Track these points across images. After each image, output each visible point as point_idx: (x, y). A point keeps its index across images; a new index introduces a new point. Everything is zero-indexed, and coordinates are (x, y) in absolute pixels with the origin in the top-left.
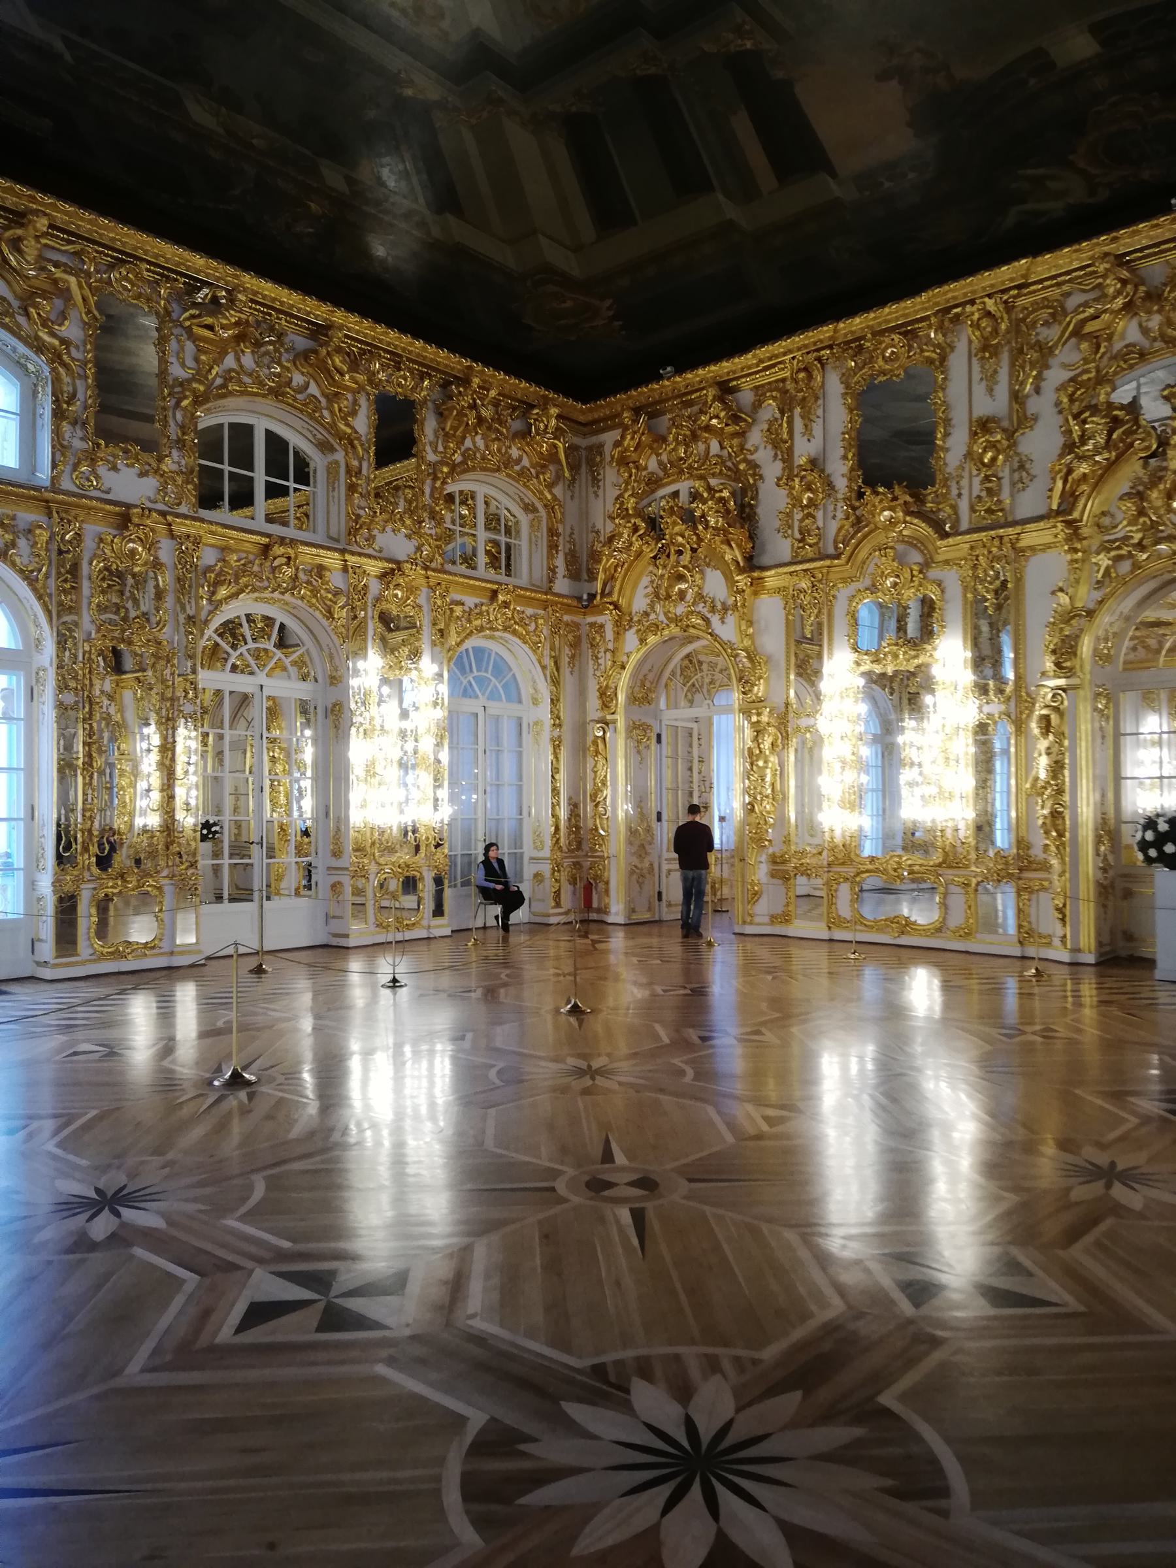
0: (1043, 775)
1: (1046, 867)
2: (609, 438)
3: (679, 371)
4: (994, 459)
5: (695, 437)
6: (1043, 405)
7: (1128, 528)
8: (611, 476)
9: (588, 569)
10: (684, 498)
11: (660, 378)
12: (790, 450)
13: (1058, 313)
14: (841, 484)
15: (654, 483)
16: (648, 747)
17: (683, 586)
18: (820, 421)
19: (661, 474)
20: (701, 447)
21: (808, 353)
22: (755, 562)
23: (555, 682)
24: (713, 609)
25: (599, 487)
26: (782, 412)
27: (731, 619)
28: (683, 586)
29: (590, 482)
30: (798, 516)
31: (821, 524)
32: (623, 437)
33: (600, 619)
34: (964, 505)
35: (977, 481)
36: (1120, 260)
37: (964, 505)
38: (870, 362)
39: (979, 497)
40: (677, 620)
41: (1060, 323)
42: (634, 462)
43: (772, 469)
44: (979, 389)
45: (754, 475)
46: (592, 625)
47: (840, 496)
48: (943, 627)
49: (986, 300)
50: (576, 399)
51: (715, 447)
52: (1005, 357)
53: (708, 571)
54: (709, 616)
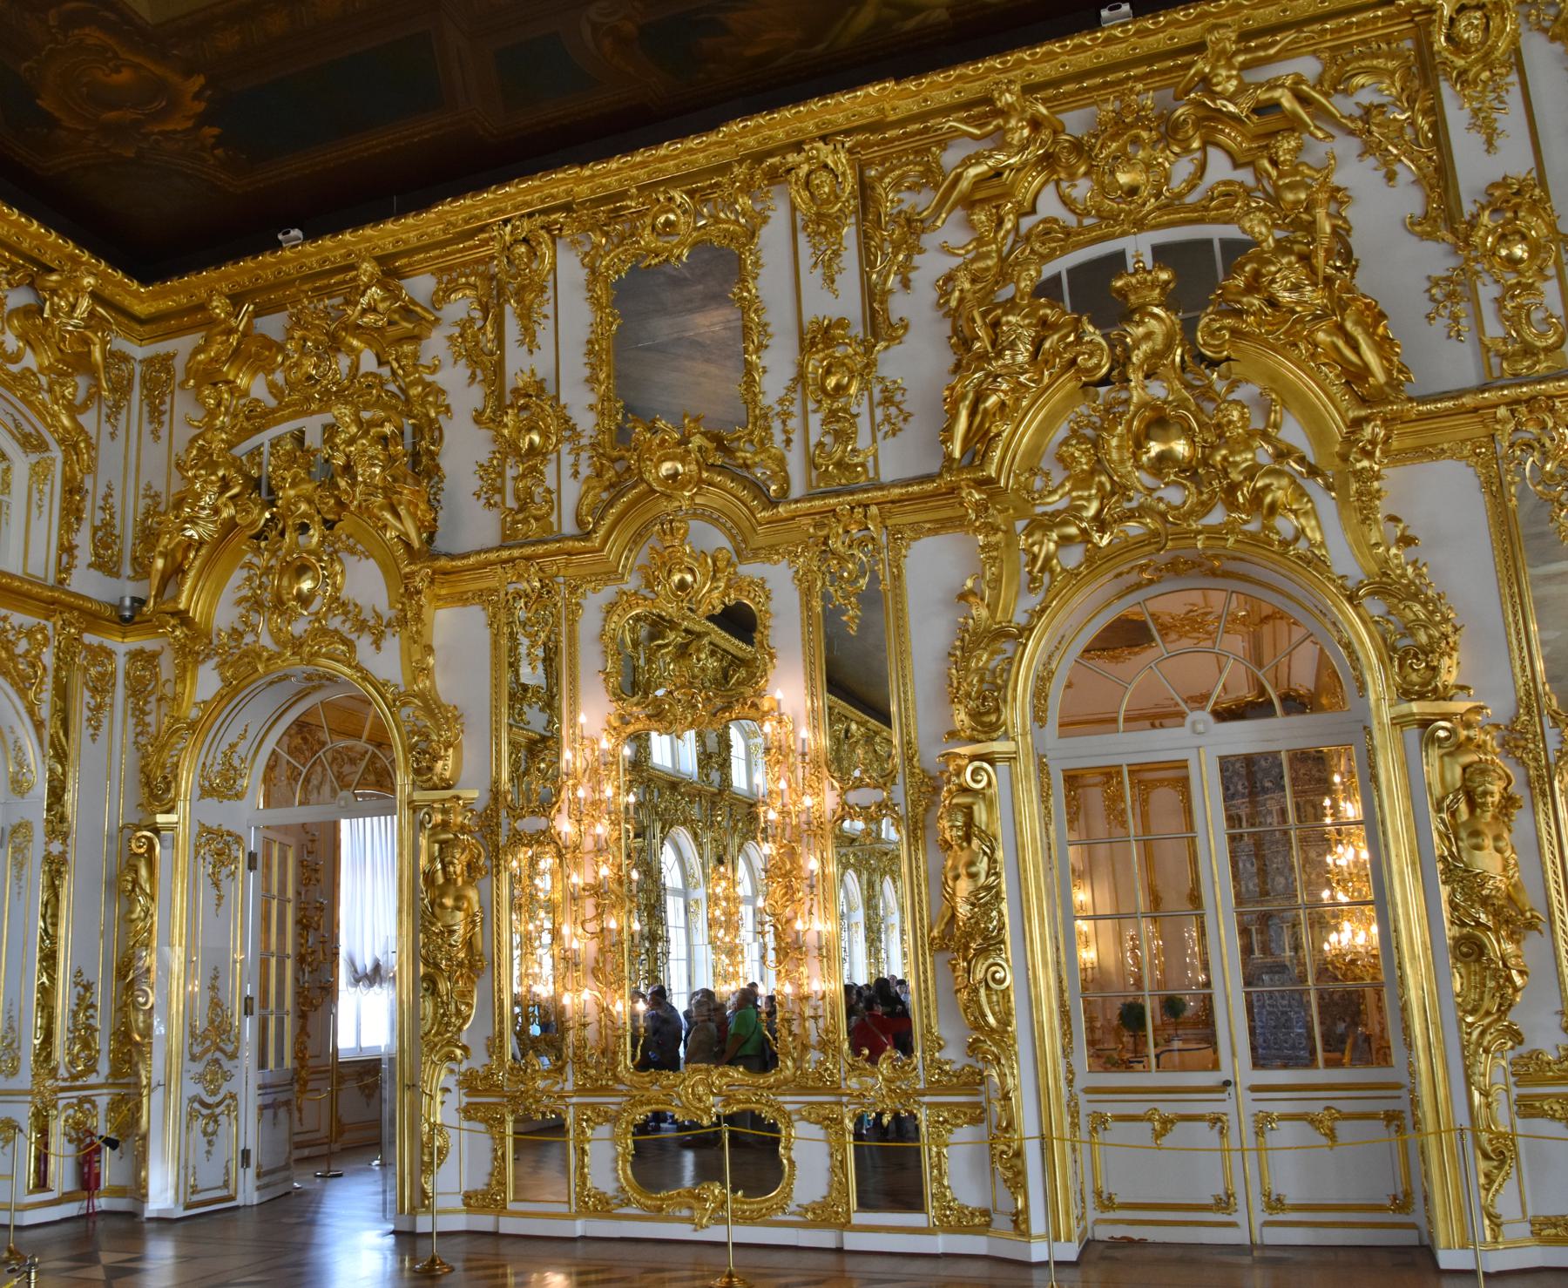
2: (182, 346)
3: (311, 235)
4: (840, 389)
5: (334, 345)
6: (914, 305)
7: (1074, 494)
8: (182, 406)
9: (135, 559)
11: (278, 245)
12: (499, 367)
13: (931, 176)
16: (233, 874)
17: (306, 585)
18: (552, 321)
19: (273, 403)
20: (343, 362)
21: (530, 215)
22: (440, 544)
23: (61, 756)
24: (362, 626)
25: (161, 423)
26: (485, 310)
27: (392, 644)
28: (306, 585)
29: (146, 415)
31: (553, 487)
33: (149, 644)
35: (815, 420)
38: (632, 235)
39: (820, 444)
41: (937, 186)
42: (227, 382)
44: (812, 280)
45: (436, 405)
47: (585, 441)
48: (772, 656)
49: (821, 145)
50: (130, 274)
51: (368, 362)
53: (350, 560)
54: (353, 637)
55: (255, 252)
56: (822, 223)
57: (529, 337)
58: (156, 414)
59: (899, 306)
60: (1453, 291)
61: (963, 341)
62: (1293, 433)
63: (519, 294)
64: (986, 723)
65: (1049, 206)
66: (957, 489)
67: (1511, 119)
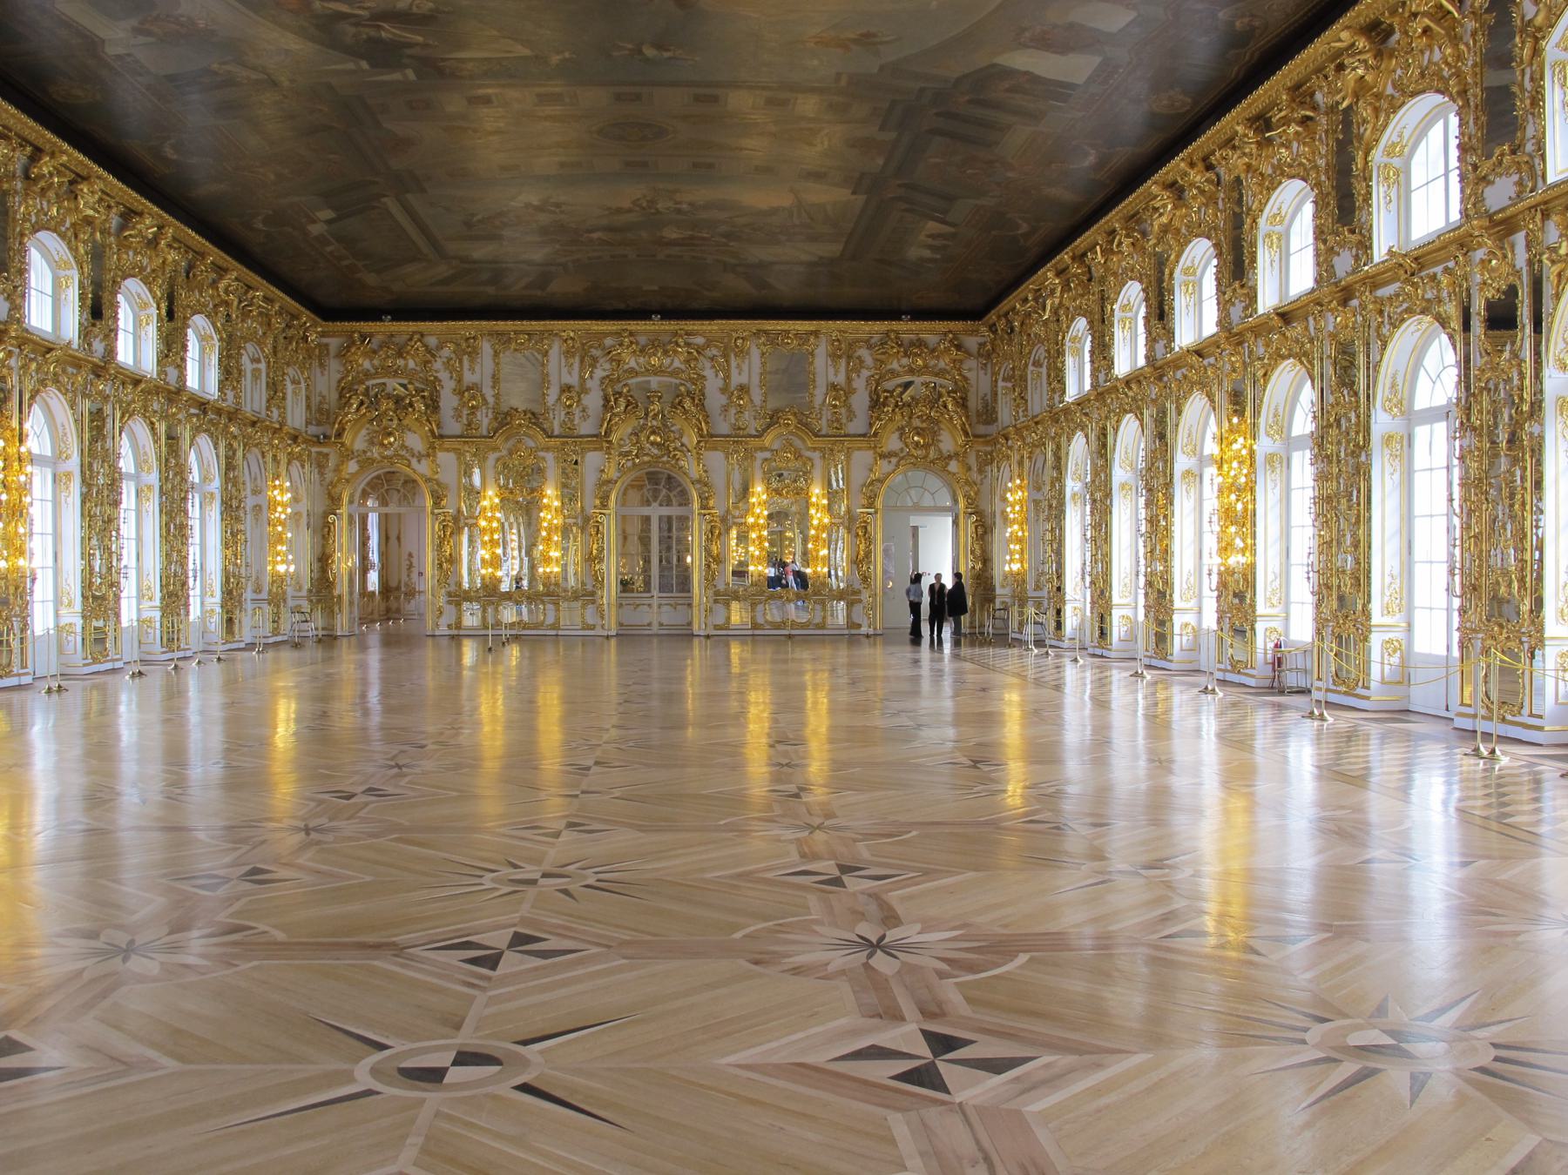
1: (593, 594)
2: (334, 343)
6: (593, 385)
8: (334, 366)
11: (381, 320)
13: (601, 346)
15: (368, 375)
30: (465, 412)
32: (348, 348)
33: (325, 450)
34: (556, 424)
36: (631, 334)
37: (556, 424)
44: (565, 370)
46: (319, 453)
51: (411, 364)
52: (577, 359)
55: (374, 320)
56: (569, 354)
57: (472, 369)
58: (322, 365)
60: (725, 409)
61: (606, 400)
62: (684, 440)
63: (469, 354)
64: (604, 506)
65: (633, 364)
66: (601, 440)
67: (745, 367)
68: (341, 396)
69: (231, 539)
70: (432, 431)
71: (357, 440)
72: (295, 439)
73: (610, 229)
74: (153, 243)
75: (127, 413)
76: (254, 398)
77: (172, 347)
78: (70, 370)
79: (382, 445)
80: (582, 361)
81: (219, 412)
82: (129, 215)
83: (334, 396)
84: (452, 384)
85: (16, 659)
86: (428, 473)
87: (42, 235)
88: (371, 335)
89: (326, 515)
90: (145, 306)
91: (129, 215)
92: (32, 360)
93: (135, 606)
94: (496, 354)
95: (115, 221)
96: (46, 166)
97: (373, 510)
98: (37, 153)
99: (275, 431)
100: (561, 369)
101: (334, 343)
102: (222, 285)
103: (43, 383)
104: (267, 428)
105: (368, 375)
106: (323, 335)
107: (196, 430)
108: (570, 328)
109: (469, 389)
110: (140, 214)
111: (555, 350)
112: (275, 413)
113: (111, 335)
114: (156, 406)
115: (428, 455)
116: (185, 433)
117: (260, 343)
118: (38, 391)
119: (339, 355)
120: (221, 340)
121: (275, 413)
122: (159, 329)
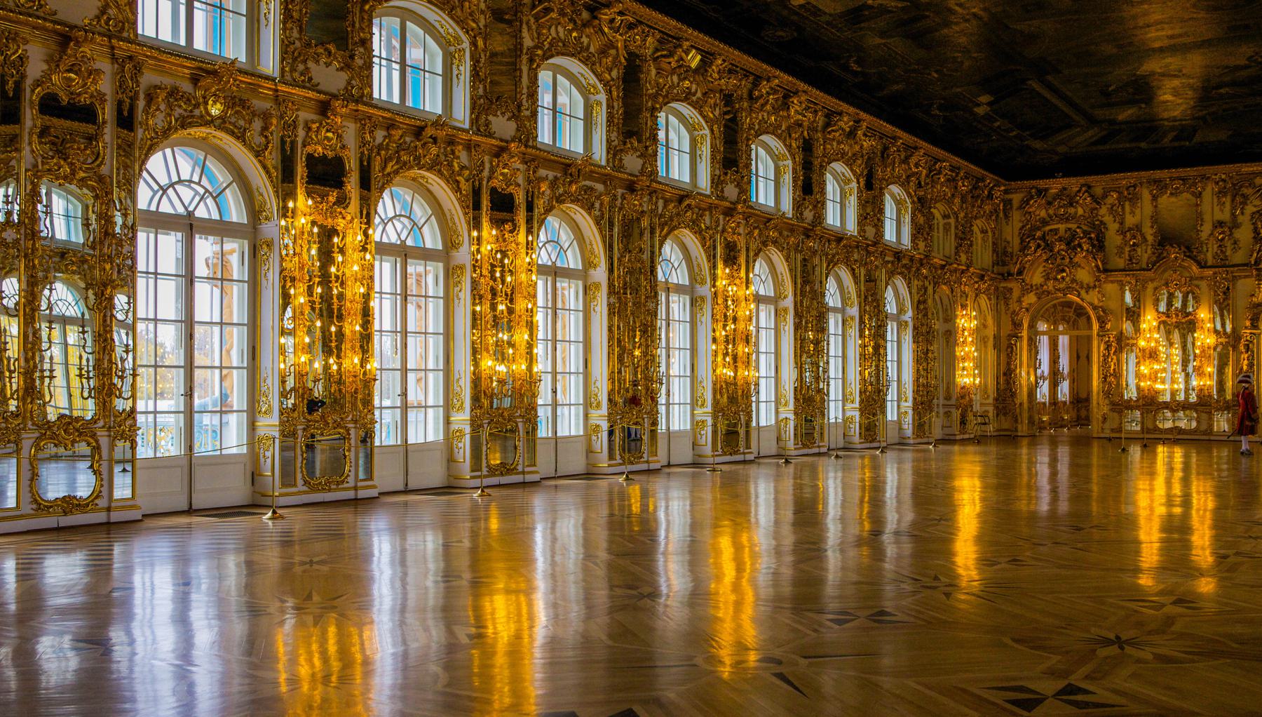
0: (1245, 368)
4: (1223, 239)
6: (1245, 219)
8: (1017, 218)
10: (1062, 232)
11: (1055, 177)
13: (1252, 185)
14: (1150, 238)
15: (1044, 222)
30: (1127, 249)
33: (1009, 285)
34: (1209, 255)
37: (1209, 255)
40: (1059, 290)
43: (1113, 227)
44: (1216, 209)
51: (1080, 211)
57: (1132, 213)
58: (1006, 216)
59: (1240, 219)
63: (1130, 200)
68: (1022, 241)
69: (922, 358)
70: (1097, 266)
71: (1037, 278)
72: (982, 277)
73: (1234, 84)
74: (851, 134)
75: (832, 263)
76: (944, 244)
77: (871, 212)
78: (785, 233)
79: (1056, 279)
80: (1233, 201)
81: (912, 259)
82: (830, 115)
83: (1017, 241)
84: (1116, 226)
85: (742, 443)
86: (1096, 302)
87: (763, 137)
88: (1046, 190)
89: (1010, 336)
90: (849, 181)
91: (830, 115)
92: (755, 228)
93: (840, 409)
94: (1155, 198)
95: (821, 120)
96: (764, 88)
97: (1062, 333)
98: (758, 79)
99: (963, 272)
100: (1213, 208)
101: (1016, 198)
102: (913, 160)
103: (765, 244)
104: (956, 270)
105: (1044, 222)
106: (1006, 192)
107: (891, 274)
108: (1221, 171)
109: (1130, 229)
110: (840, 114)
111: (1209, 191)
112: (963, 258)
113: (819, 206)
114: (856, 256)
115: (1095, 287)
116: (882, 275)
117: (950, 202)
118: (760, 250)
119: (1020, 208)
120: (913, 202)
121: (963, 258)
122: (859, 198)
